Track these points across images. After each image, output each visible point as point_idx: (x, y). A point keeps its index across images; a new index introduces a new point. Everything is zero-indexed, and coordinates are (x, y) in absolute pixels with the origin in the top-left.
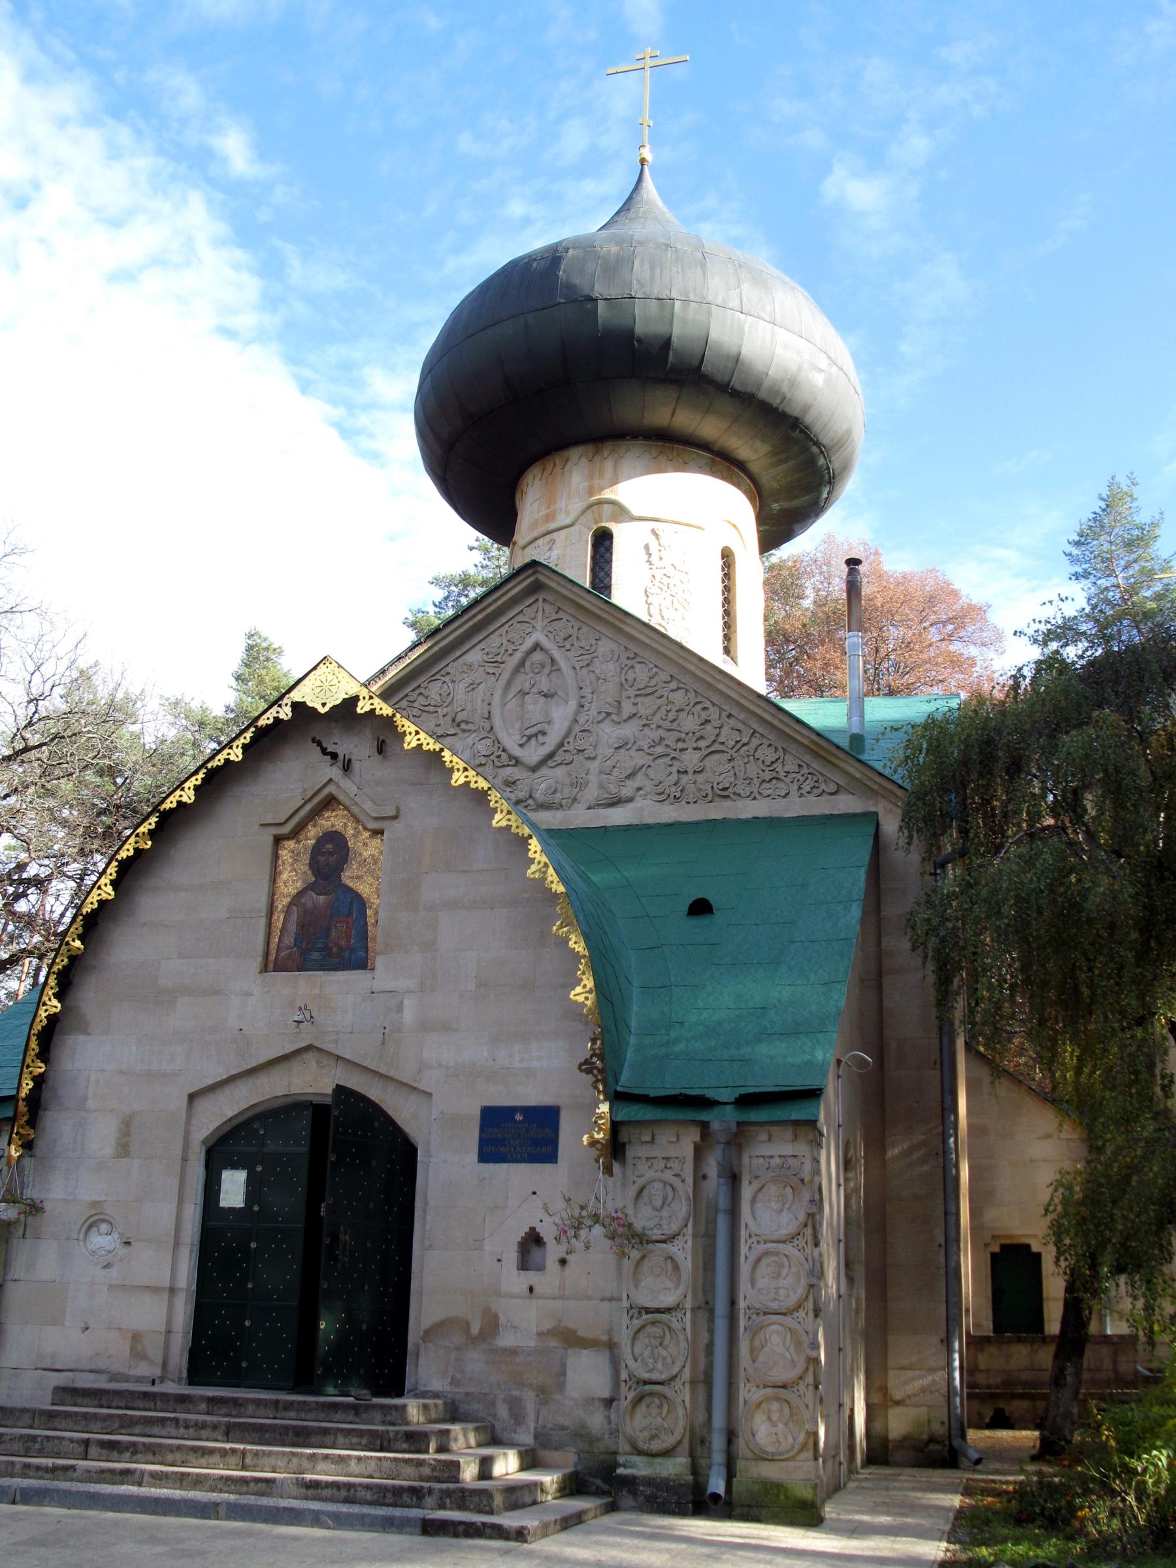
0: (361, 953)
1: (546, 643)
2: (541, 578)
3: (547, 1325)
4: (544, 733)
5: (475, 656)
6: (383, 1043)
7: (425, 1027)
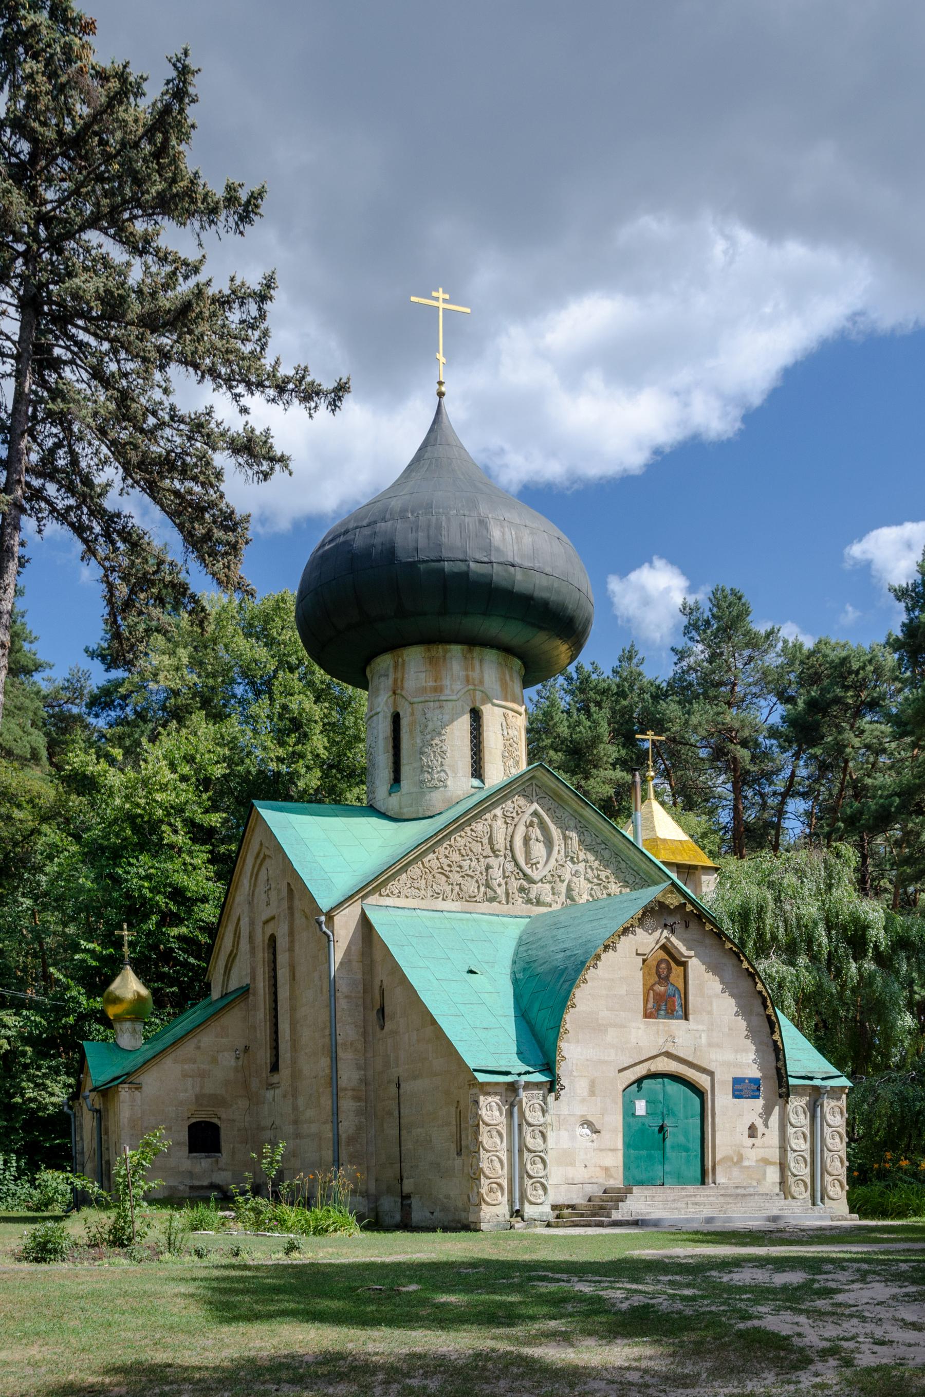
5: (498, 811)
7: (710, 1045)
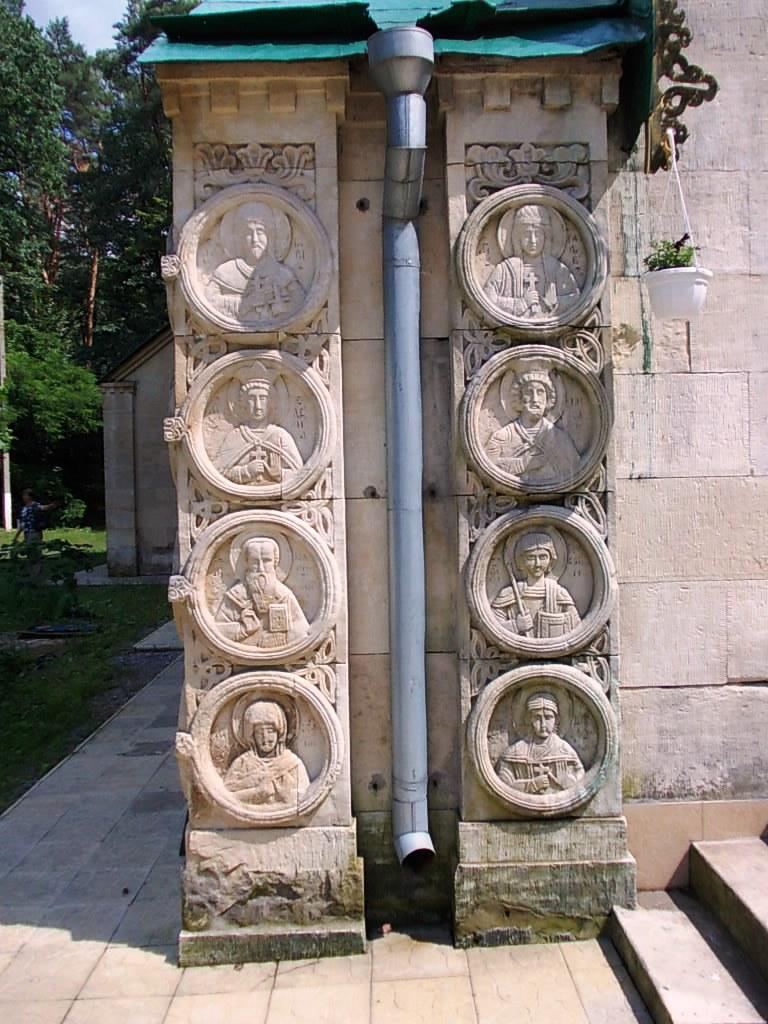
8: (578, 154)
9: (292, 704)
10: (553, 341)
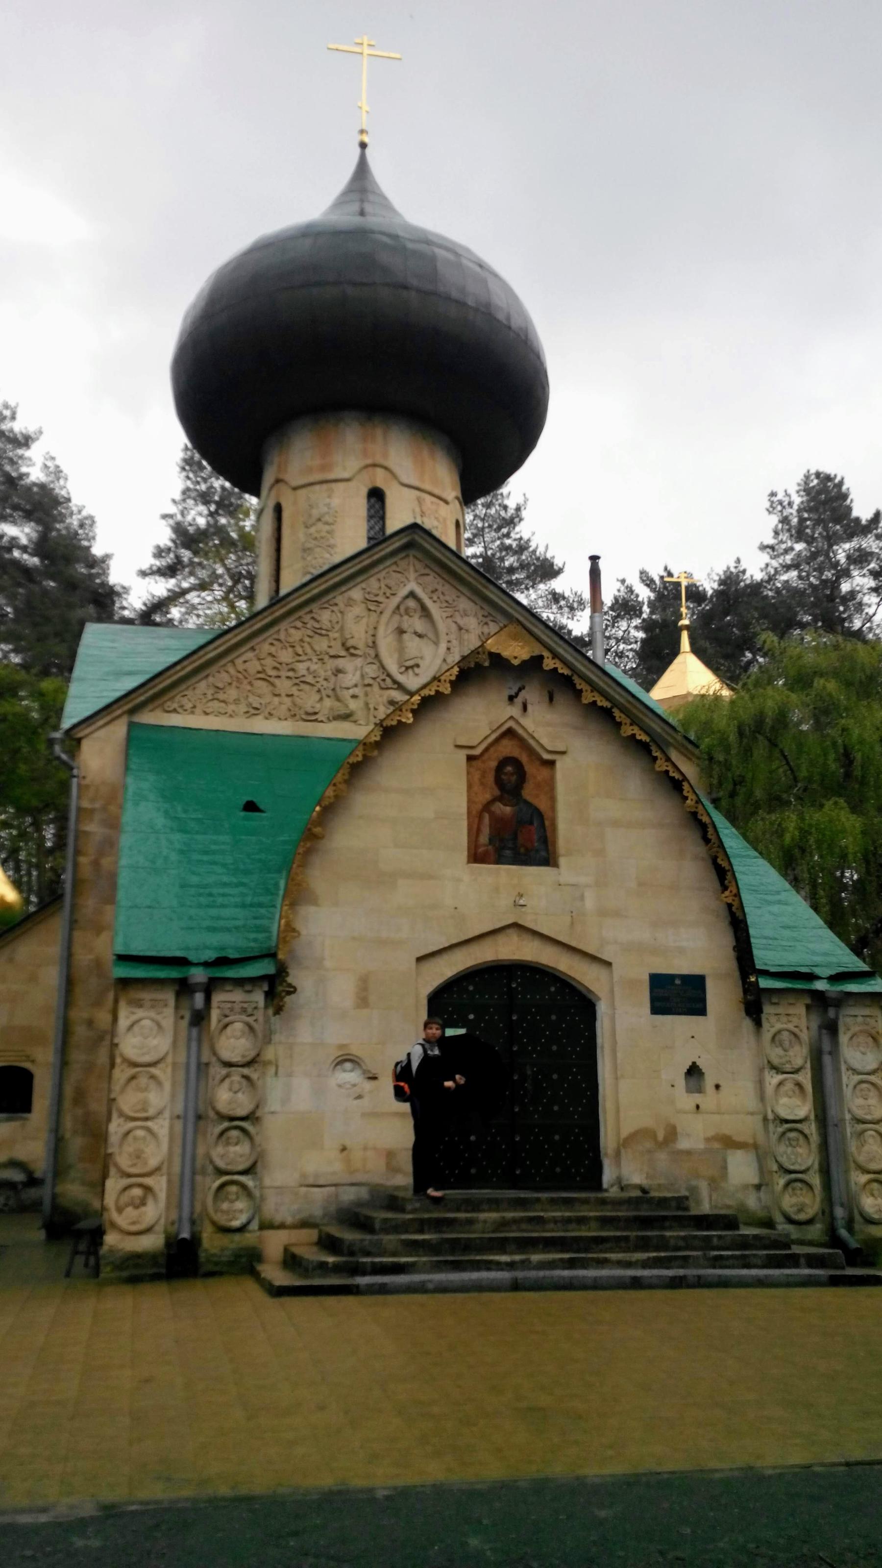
0: (543, 853)
1: (419, 591)
2: (417, 538)
3: (711, 1133)
4: (418, 666)
5: (356, 594)
6: (572, 923)
7: (603, 913)
8: (254, 1005)
9: (148, 1189)
10: (243, 1066)
